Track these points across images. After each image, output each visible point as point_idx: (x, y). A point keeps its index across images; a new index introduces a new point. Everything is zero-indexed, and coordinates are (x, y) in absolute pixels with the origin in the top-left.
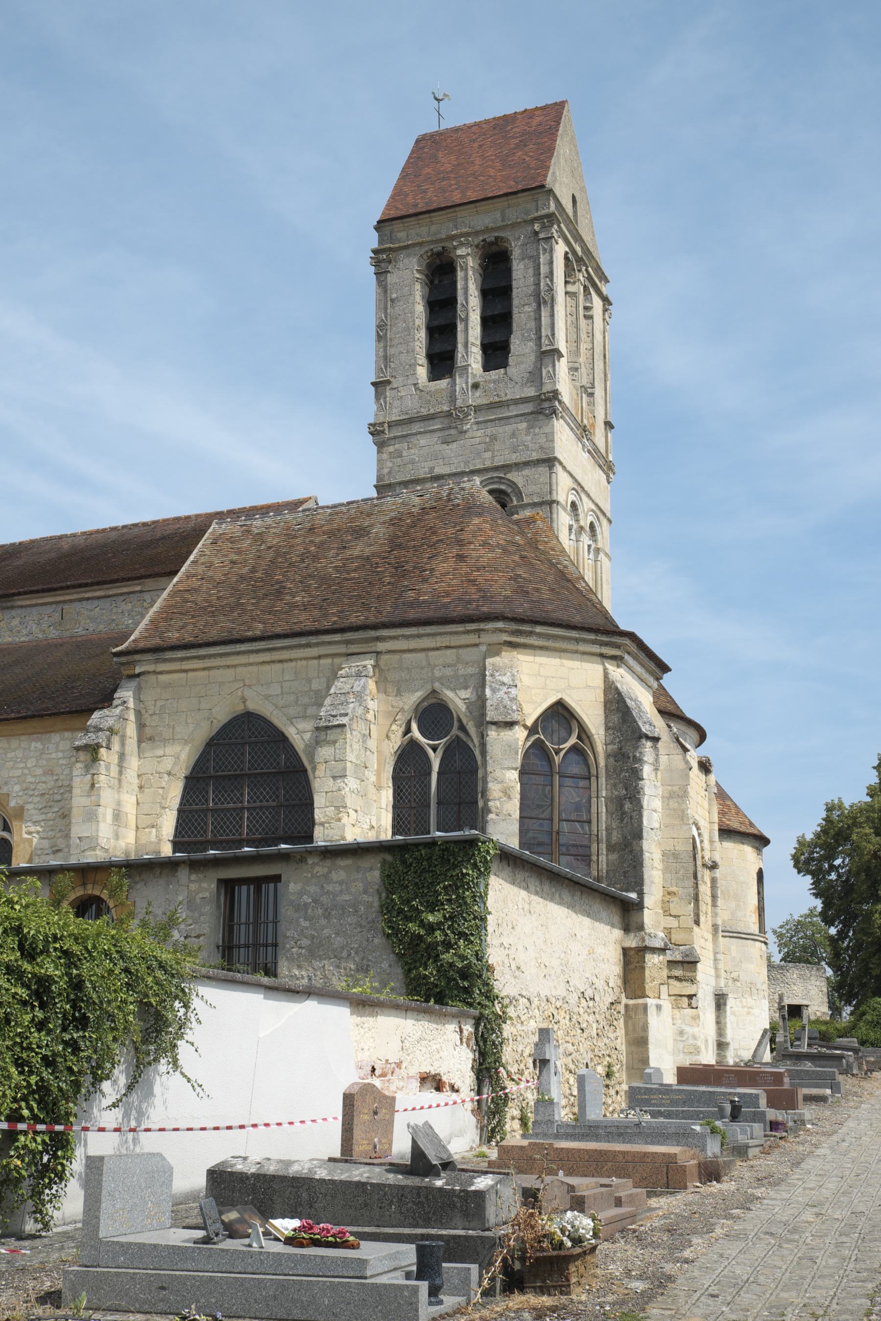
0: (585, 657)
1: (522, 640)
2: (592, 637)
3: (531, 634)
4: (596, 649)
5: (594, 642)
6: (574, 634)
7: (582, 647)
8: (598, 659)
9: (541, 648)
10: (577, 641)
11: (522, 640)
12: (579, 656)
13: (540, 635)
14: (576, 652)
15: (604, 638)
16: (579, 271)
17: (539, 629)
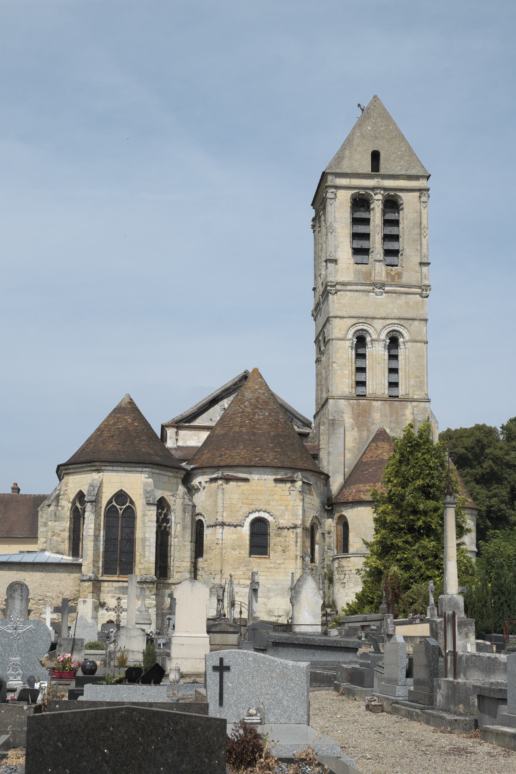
0: (88, 472)
1: (68, 471)
2: (85, 465)
3: (70, 469)
4: (89, 469)
5: (88, 466)
6: (80, 466)
7: (85, 469)
8: (92, 472)
9: (75, 472)
10: (83, 467)
11: (68, 471)
12: (85, 472)
13: (72, 468)
14: (84, 471)
15: (89, 465)
16: (375, 194)
17: (70, 467)
